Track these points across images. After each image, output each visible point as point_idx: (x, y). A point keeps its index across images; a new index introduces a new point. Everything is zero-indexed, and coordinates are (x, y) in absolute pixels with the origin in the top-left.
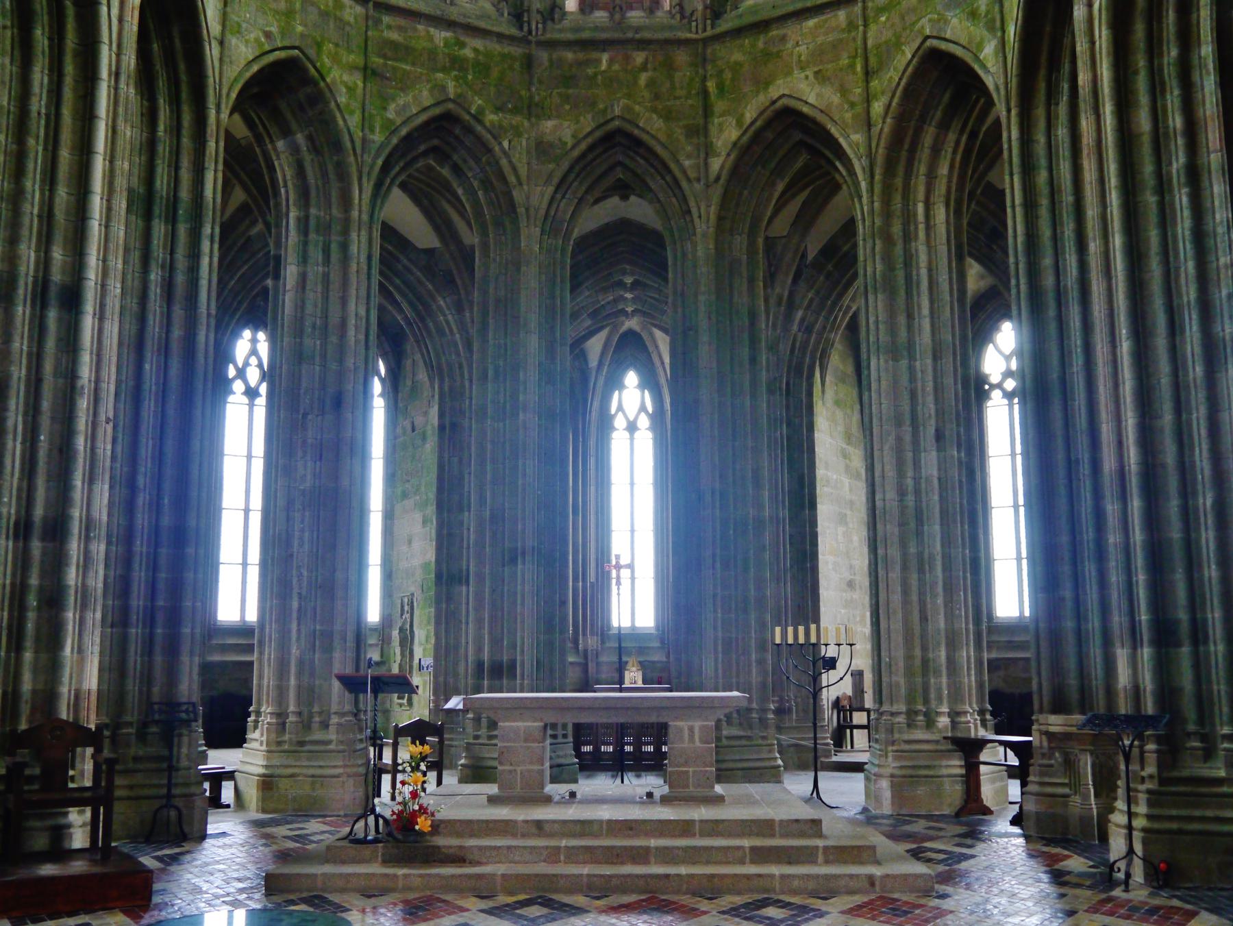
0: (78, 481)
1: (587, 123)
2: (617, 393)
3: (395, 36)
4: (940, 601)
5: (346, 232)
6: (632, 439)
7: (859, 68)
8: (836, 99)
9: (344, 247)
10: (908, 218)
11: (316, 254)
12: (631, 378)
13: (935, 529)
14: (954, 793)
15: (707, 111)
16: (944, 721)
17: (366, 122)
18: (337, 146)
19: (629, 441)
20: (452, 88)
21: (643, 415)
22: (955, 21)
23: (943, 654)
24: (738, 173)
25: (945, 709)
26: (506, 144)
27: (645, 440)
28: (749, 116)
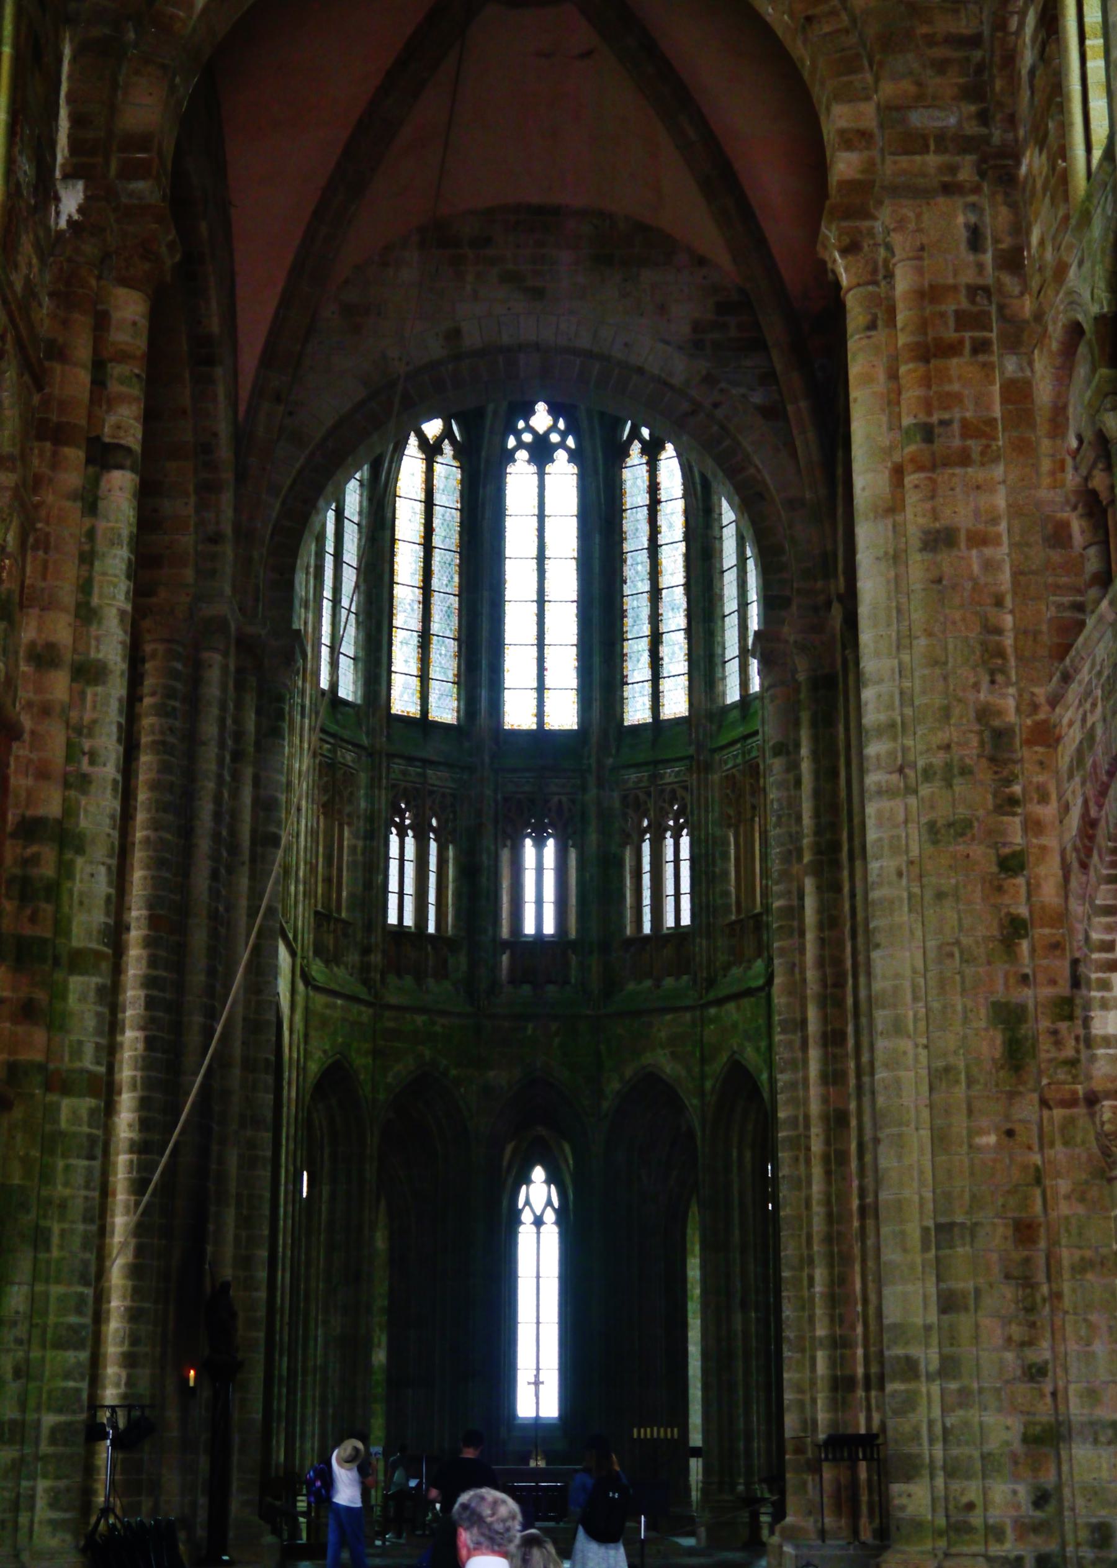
0: (277, 1357)
2: (524, 1187)
3: (391, 1024)
4: (741, 1411)
6: (538, 1233)
7: (698, 1054)
8: (683, 1073)
12: (538, 1173)
13: (739, 1364)
16: (741, 1488)
19: (535, 1236)
20: (428, 1053)
21: (549, 1209)
22: (749, 1049)
23: (741, 1445)
25: (741, 1481)
26: (462, 1090)
27: (551, 1234)
28: (628, 1073)
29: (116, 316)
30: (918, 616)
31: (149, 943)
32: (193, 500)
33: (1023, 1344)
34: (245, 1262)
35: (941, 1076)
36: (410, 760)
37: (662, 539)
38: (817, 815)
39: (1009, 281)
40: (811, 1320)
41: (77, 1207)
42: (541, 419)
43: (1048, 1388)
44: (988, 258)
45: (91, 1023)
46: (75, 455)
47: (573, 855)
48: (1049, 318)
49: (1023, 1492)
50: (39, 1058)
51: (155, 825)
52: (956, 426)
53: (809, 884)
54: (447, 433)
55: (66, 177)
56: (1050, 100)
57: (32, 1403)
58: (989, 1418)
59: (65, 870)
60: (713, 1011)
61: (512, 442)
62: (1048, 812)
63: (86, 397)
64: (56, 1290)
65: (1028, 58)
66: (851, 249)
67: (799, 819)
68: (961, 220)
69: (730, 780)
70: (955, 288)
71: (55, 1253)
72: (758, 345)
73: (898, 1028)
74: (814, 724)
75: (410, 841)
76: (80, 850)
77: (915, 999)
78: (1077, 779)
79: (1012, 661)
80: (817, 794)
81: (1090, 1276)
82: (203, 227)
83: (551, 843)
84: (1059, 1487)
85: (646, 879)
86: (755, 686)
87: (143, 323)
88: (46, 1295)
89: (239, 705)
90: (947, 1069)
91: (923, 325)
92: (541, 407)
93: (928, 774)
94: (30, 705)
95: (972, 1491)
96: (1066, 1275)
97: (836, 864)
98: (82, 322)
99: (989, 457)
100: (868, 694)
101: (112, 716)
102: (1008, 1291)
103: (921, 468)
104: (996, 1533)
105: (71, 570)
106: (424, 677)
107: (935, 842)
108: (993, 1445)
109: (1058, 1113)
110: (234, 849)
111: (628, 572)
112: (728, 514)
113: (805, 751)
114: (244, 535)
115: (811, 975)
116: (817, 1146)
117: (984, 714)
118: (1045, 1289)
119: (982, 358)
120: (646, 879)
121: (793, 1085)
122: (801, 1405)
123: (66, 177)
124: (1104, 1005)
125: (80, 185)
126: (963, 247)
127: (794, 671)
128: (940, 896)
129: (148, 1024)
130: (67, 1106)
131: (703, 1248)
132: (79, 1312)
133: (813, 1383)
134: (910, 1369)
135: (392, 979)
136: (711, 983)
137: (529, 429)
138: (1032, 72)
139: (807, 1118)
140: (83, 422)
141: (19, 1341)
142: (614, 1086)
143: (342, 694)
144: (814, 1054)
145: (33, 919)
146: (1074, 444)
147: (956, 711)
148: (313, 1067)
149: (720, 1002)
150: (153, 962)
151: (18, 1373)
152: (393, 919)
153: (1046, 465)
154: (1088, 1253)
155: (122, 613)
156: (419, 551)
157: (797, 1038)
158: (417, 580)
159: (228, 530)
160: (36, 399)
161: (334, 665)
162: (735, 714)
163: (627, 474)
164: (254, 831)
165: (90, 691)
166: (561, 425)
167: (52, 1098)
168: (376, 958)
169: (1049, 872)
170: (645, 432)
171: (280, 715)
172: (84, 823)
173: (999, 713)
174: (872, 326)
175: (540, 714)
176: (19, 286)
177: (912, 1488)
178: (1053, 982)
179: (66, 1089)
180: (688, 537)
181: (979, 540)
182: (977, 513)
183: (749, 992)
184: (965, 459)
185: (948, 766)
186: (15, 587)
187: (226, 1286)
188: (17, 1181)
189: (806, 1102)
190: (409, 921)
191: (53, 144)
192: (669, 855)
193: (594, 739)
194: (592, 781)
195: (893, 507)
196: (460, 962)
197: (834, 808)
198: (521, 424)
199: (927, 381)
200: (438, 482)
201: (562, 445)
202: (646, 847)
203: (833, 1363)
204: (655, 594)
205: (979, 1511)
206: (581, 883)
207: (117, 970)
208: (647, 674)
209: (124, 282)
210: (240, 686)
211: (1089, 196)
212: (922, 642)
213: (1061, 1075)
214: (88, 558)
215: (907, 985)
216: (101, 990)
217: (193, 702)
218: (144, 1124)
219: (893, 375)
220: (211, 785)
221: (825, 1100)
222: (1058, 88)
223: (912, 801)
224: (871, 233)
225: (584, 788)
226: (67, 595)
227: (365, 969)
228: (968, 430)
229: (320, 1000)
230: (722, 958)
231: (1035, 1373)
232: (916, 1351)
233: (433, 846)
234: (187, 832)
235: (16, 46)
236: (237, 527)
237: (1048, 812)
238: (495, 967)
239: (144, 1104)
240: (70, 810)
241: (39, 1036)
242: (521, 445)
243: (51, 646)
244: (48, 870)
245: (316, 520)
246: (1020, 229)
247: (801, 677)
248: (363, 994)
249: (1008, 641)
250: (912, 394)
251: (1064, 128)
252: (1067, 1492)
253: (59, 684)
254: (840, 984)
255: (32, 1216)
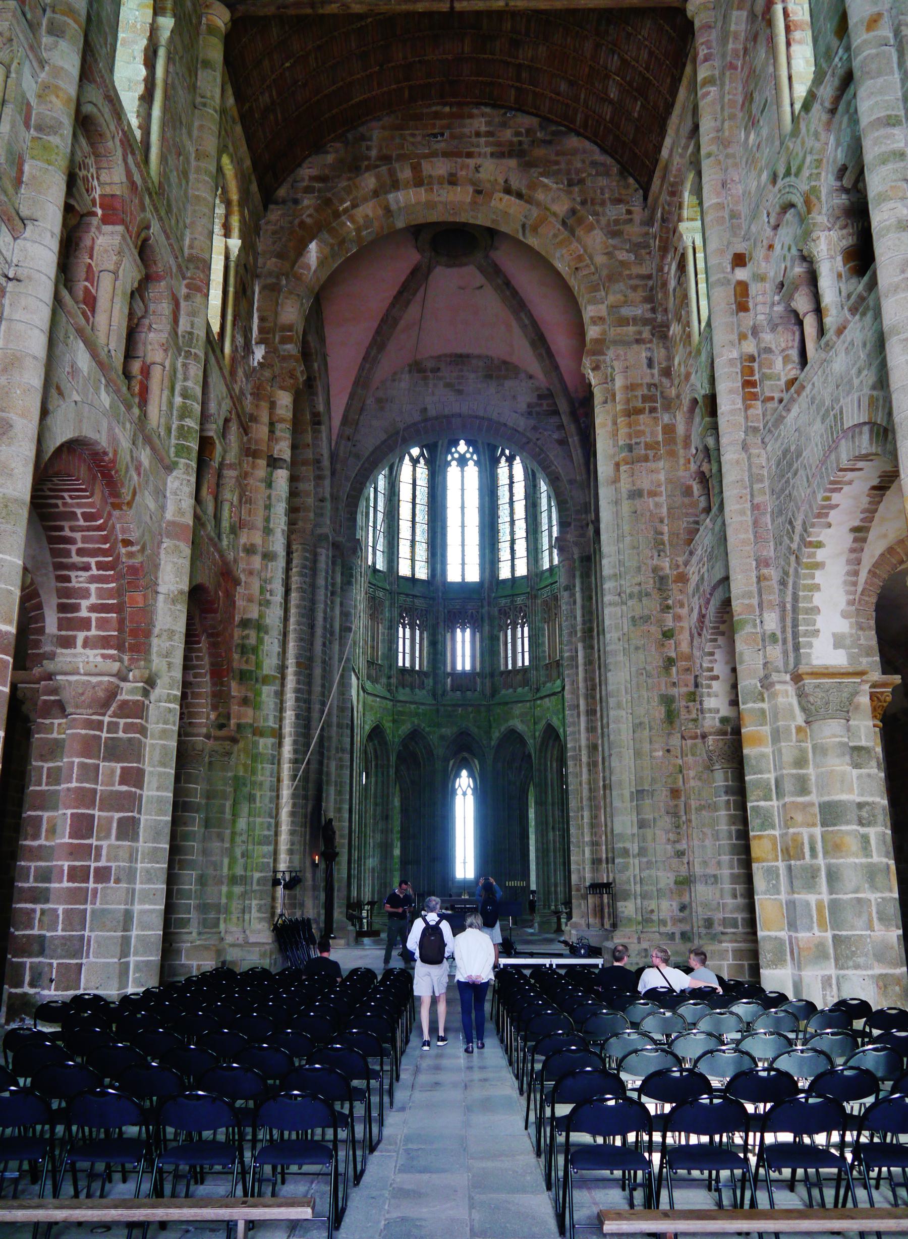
1: (455, 729)
5: (388, 768)
9: (388, 772)
10: (546, 765)
11: (380, 775)
12: (464, 773)
13: (552, 854)
14: (554, 926)
15: (490, 727)
17: (394, 736)
18: (386, 743)
20: (416, 721)
24: (499, 746)
27: (470, 800)
28: (502, 729)
29: (279, 403)
30: (626, 528)
31: (297, 674)
32: (312, 483)
33: (674, 842)
34: (339, 810)
35: (638, 726)
36: (407, 595)
37: (515, 499)
38: (583, 616)
39: (665, 381)
40: (583, 833)
41: (267, 785)
42: (462, 447)
43: (685, 861)
44: (656, 371)
45: (272, 706)
46: (262, 463)
47: (478, 635)
48: (683, 397)
49: (675, 905)
50: (250, 721)
51: (299, 623)
52: (642, 445)
53: (580, 646)
54: (422, 454)
55: (257, 343)
56: (682, 302)
57: (249, 868)
58: (660, 874)
59: (260, 641)
60: (539, 702)
61: (449, 458)
62: (684, 612)
63: (266, 438)
64: (259, 820)
65: (672, 283)
66: (596, 368)
67: (575, 618)
68: (644, 355)
69: (545, 603)
70: (641, 385)
71: (258, 804)
72: (556, 413)
73: (619, 706)
74: (582, 577)
75: (408, 630)
76: (266, 633)
77: (626, 692)
78: (696, 597)
79: (668, 546)
80: (583, 607)
81: (704, 812)
82: (316, 365)
83: (468, 630)
84: (690, 903)
85: (509, 646)
86: (556, 562)
87: (291, 406)
88: (254, 822)
89: (333, 572)
90: (641, 724)
91: (628, 401)
92: (462, 442)
93: (631, 596)
94: (244, 570)
95: (653, 905)
96: (693, 812)
97: (592, 637)
98: (264, 405)
99: (656, 458)
100: (605, 562)
101: (280, 575)
102: (668, 819)
103: (627, 463)
104: (663, 922)
105: (261, 513)
106: (413, 560)
107: (634, 626)
108: (662, 885)
109: (689, 742)
110: (332, 633)
111: (501, 513)
112: (543, 487)
113: (578, 589)
114: (334, 498)
115: (581, 685)
116: (584, 759)
117: (655, 570)
118: (684, 818)
119: (654, 415)
120: (509, 646)
121: (574, 733)
122: (579, 871)
123: (257, 343)
124: (709, 695)
125: (263, 346)
126: (645, 366)
127: (573, 554)
128: (637, 648)
129: (297, 708)
130: (262, 741)
131: (536, 803)
132: (269, 830)
133: (584, 861)
134: (625, 852)
135: (401, 689)
136: (538, 690)
137: (457, 452)
138: (674, 290)
139: (580, 747)
140: (265, 449)
141: (243, 842)
142: (496, 735)
143: (378, 567)
144: (583, 719)
145: (247, 662)
146: (694, 451)
147: (643, 569)
148: (367, 728)
149: (541, 698)
150: (298, 682)
151: (243, 856)
152: (400, 664)
153: (682, 461)
154: (703, 803)
155: (283, 531)
156: (410, 505)
157: (575, 712)
158: (410, 518)
159: (328, 496)
160: (245, 439)
161: (374, 554)
162: (547, 574)
163: (499, 471)
164: (341, 625)
165: (270, 564)
166: (471, 450)
167: (256, 738)
168: (394, 681)
169: (684, 638)
170: (507, 452)
171: (351, 576)
172: (268, 621)
173: (662, 569)
174: (605, 402)
175: (463, 575)
176: (237, 391)
177: (626, 904)
178: (687, 685)
179: (262, 735)
180: (526, 498)
181: (653, 494)
182: (652, 482)
183: (554, 694)
184: (646, 459)
185: (640, 592)
186: (237, 519)
187: (331, 820)
188: (241, 774)
189: (579, 740)
190: (407, 664)
191: (251, 330)
192: (519, 635)
193: (486, 585)
194: (485, 603)
195: (616, 480)
196: (429, 682)
197: (591, 613)
198: (453, 450)
199: (630, 425)
200: (418, 475)
201: (471, 458)
202: (509, 632)
203: (592, 852)
204: (512, 522)
205: (656, 913)
206: (481, 646)
207: (283, 685)
208: (509, 557)
209: (282, 388)
210: (334, 563)
211: (700, 343)
212: (628, 539)
213: (691, 725)
214: (268, 507)
215: (623, 687)
216: (276, 693)
217: (314, 571)
218: (295, 751)
219: (615, 423)
220: (322, 606)
221: (588, 739)
222: (685, 296)
223: (624, 607)
224: (605, 362)
225: (482, 607)
226: (260, 523)
227: (389, 685)
228: (648, 446)
229: (370, 699)
230: (543, 679)
231: (680, 854)
232: (628, 845)
233: (418, 632)
234: (312, 627)
235: (235, 287)
236: (332, 495)
237: (684, 612)
238: (445, 683)
239: (295, 742)
240: (262, 616)
241: (250, 712)
242: (453, 459)
243: (253, 545)
244: (252, 641)
245: (365, 492)
246: (670, 358)
247: (576, 557)
248: (388, 696)
249: (666, 538)
250: (623, 431)
251: (688, 313)
252: (694, 905)
253: (257, 561)
254: (593, 689)
255: (248, 788)
